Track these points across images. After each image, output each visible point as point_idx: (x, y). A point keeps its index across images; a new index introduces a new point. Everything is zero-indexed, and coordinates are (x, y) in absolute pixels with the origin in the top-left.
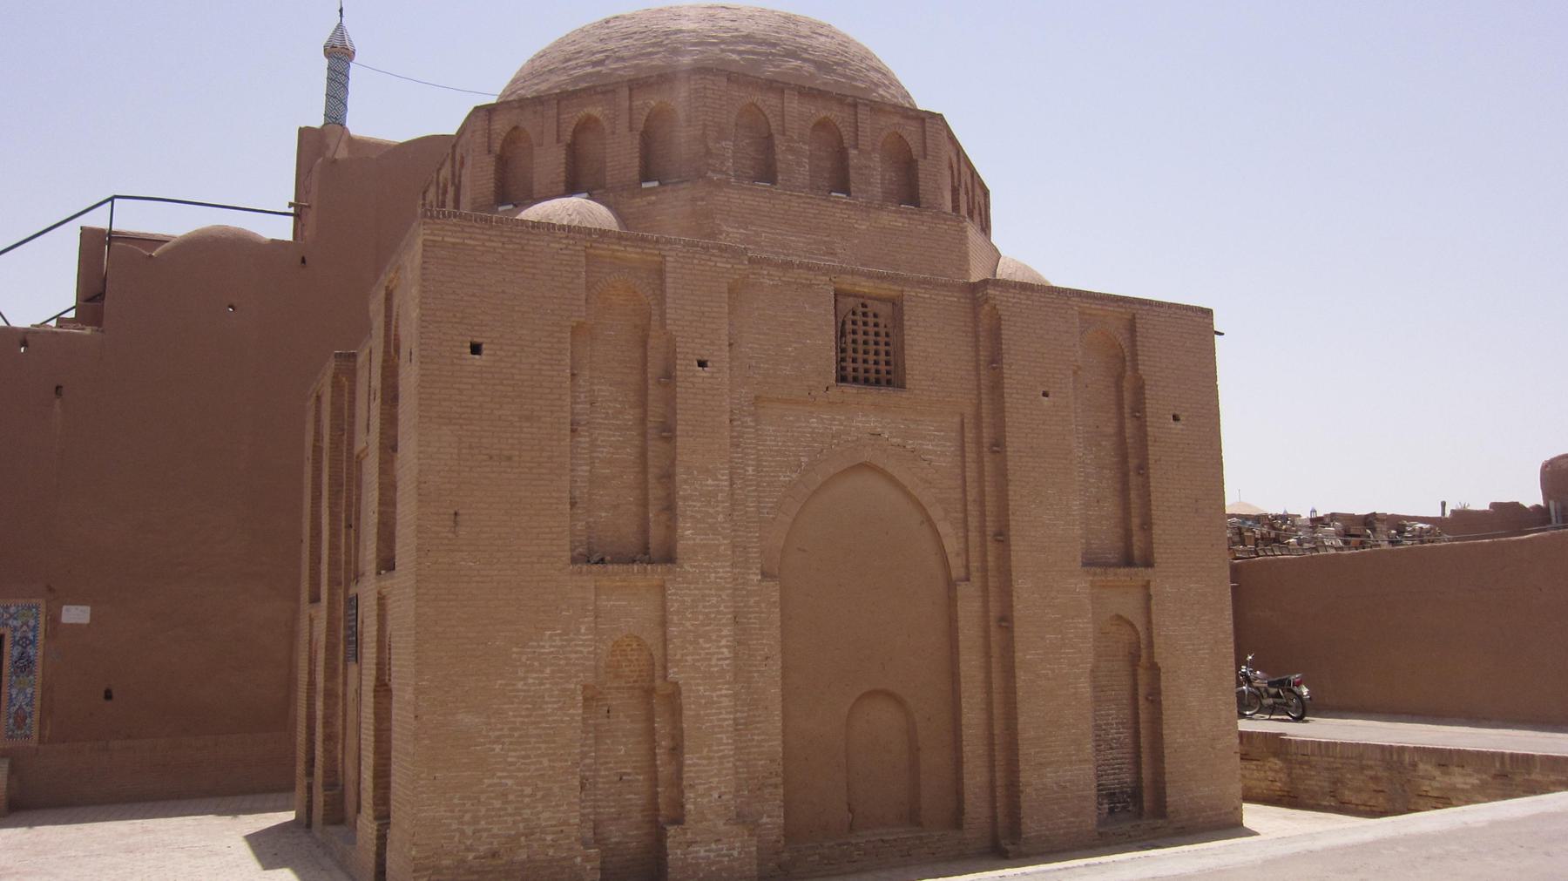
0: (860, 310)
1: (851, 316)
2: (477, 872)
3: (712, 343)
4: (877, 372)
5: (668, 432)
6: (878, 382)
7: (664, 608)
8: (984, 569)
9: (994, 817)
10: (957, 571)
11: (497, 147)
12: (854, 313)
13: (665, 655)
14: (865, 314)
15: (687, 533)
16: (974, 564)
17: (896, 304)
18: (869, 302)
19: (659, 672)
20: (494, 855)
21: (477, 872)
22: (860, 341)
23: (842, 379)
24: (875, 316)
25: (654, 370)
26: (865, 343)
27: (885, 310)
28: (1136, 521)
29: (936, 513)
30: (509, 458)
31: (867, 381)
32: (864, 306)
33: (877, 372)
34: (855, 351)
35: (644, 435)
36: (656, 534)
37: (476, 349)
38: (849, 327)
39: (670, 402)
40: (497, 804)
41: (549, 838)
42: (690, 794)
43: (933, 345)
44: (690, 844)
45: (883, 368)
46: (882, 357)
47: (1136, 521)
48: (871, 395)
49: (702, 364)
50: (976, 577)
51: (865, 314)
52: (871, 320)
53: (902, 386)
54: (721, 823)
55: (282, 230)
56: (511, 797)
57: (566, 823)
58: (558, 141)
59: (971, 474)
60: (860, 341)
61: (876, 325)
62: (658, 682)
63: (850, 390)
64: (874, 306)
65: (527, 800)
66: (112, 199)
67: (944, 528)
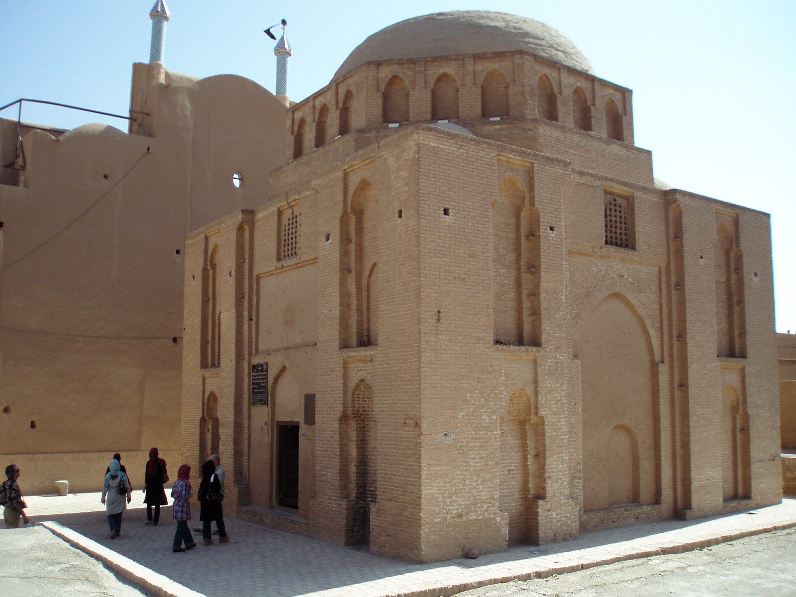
0: (613, 202)
1: (609, 206)
2: (451, 526)
3: (556, 217)
4: (621, 239)
5: (534, 268)
6: (621, 246)
7: (536, 373)
8: (671, 356)
9: (675, 497)
10: (657, 358)
11: (383, 88)
12: (611, 205)
13: (536, 401)
14: (615, 205)
15: (547, 328)
16: (666, 354)
17: (630, 201)
18: (616, 198)
19: (533, 410)
20: (460, 516)
21: (451, 526)
22: (613, 221)
23: (606, 243)
24: (620, 206)
25: (524, 231)
26: (616, 222)
27: (622, 202)
28: (736, 332)
29: (648, 322)
30: (464, 279)
31: (616, 245)
32: (615, 200)
33: (621, 239)
34: (611, 227)
35: (518, 269)
36: (527, 329)
37: (446, 212)
38: (608, 212)
39: (535, 251)
40: (461, 486)
41: (485, 506)
42: (549, 482)
43: (648, 227)
44: (549, 510)
45: (623, 237)
46: (623, 231)
47: (736, 332)
48: (620, 252)
49: (552, 229)
50: (666, 360)
51: (615, 205)
52: (618, 209)
53: (634, 248)
54: (562, 498)
55: (123, 126)
56: (467, 482)
57: (493, 498)
58: (426, 87)
59: (664, 302)
60: (613, 221)
61: (620, 212)
62: (533, 416)
63: (612, 249)
64: (620, 201)
65: (474, 484)
66: (20, 101)
67: (652, 332)
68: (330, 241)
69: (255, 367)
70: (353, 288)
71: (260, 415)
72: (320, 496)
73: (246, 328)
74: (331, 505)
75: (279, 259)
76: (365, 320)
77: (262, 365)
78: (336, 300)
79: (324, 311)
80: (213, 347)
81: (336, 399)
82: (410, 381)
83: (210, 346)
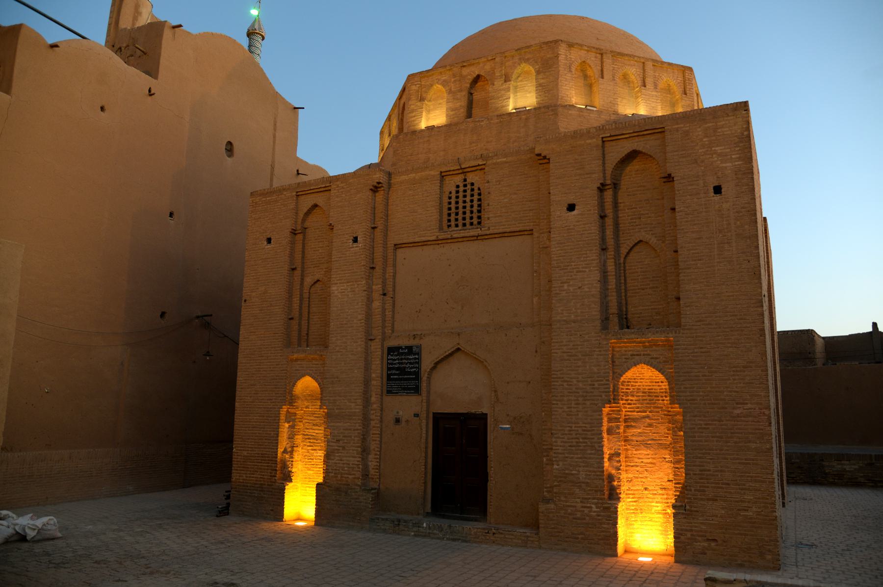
68: (575, 212)
69: (391, 350)
70: (611, 267)
71: (406, 405)
72: (563, 498)
73: (376, 304)
74: (586, 511)
75: (441, 229)
76: (624, 302)
77: (410, 348)
78: (596, 276)
79: (566, 287)
80: (300, 325)
81: (596, 386)
82: (744, 367)
83: (295, 323)
